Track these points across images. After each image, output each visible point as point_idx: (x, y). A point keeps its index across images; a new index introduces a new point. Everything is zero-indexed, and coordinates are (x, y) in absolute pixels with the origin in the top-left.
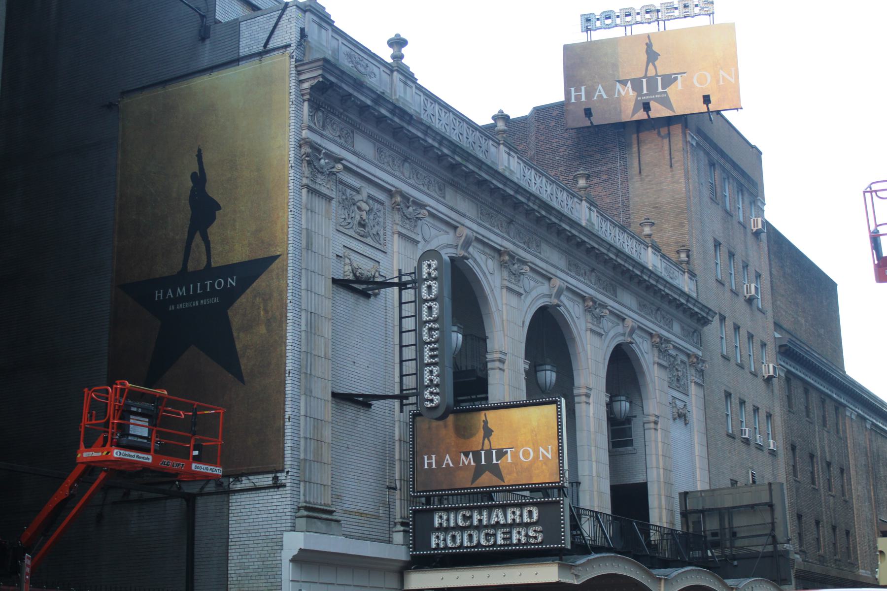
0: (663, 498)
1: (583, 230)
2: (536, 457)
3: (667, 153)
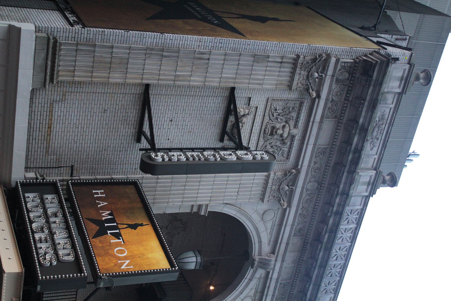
2: (120, 259)
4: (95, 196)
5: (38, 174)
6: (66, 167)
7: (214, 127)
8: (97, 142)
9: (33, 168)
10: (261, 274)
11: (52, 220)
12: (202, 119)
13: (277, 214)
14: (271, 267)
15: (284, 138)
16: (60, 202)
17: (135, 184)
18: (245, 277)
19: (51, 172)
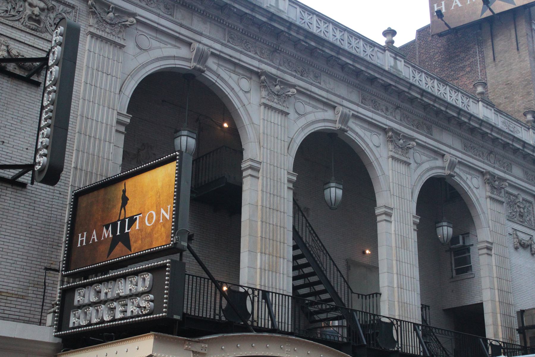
0: (499, 315)
1: (370, 66)
2: (158, 220)
3: (514, 40)
4: (84, 244)
5: (50, 311)
6: (45, 276)
7: (18, 91)
8: (18, 236)
9: (41, 316)
10: (214, 63)
11: (103, 297)
12: (6, 105)
13: (143, 32)
14: (206, 49)
15: (46, 7)
16: (84, 286)
17: (78, 196)
18: (214, 82)
19: (50, 295)
